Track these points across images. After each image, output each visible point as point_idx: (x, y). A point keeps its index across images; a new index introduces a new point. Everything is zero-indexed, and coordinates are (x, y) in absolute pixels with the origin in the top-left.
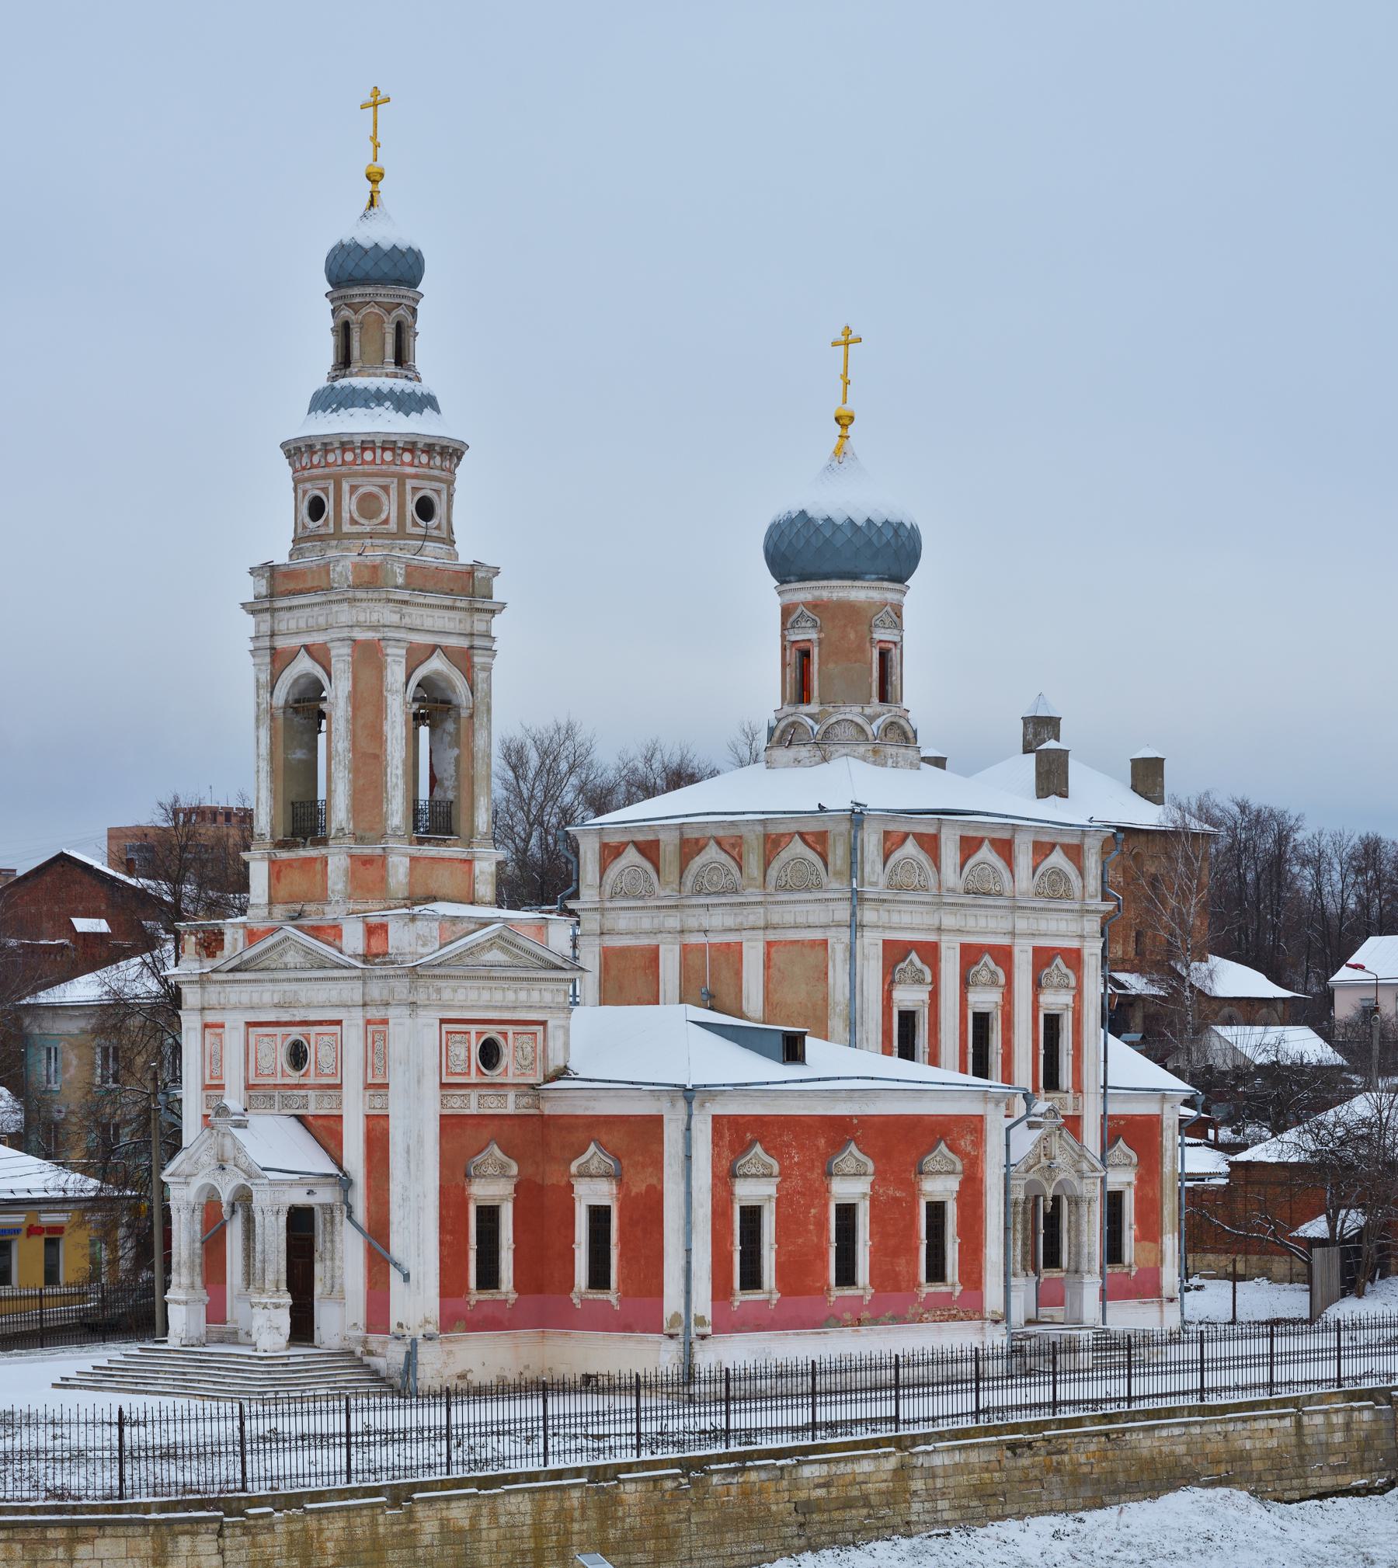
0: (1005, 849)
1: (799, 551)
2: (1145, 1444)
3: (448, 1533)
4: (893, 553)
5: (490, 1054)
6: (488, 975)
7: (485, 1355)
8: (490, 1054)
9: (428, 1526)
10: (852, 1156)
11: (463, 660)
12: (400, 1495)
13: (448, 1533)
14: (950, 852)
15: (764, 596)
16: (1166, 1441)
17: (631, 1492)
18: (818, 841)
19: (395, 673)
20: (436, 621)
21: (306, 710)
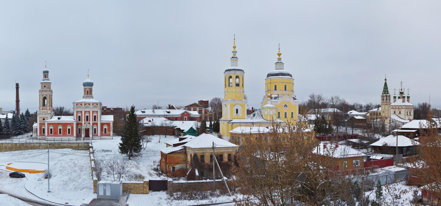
0: (89, 104)
1: (85, 85)
2: (62, 145)
3: (5, 146)
4: (91, 84)
5: (44, 119)
6: (43, 114)
7: (41, 137)
8: (44, 119)
9: (4, 145)
10: (60, 125)
11: (47, 95)
12: (2, 144)
13: (5, 146)
14: (83, 105)
15: (83, 88)
16: (65, 145)
17: (18, 145)
18: (97, 104)
19: (41, 97)
20: (50, 93)
21: (45, 98)
